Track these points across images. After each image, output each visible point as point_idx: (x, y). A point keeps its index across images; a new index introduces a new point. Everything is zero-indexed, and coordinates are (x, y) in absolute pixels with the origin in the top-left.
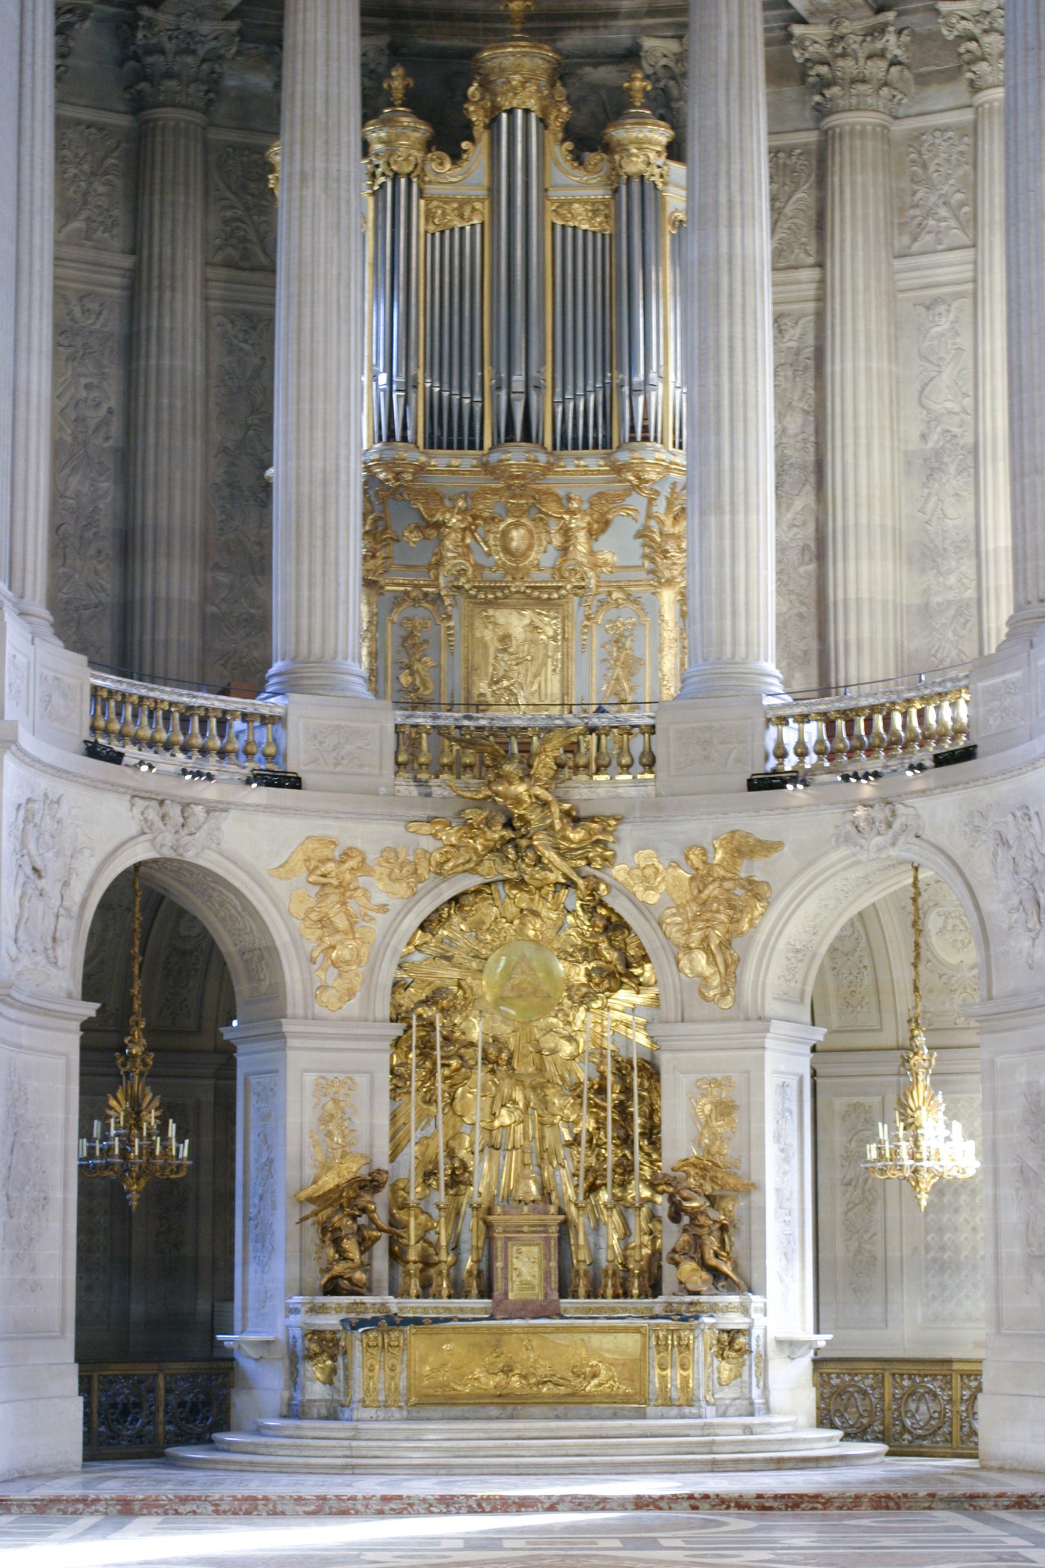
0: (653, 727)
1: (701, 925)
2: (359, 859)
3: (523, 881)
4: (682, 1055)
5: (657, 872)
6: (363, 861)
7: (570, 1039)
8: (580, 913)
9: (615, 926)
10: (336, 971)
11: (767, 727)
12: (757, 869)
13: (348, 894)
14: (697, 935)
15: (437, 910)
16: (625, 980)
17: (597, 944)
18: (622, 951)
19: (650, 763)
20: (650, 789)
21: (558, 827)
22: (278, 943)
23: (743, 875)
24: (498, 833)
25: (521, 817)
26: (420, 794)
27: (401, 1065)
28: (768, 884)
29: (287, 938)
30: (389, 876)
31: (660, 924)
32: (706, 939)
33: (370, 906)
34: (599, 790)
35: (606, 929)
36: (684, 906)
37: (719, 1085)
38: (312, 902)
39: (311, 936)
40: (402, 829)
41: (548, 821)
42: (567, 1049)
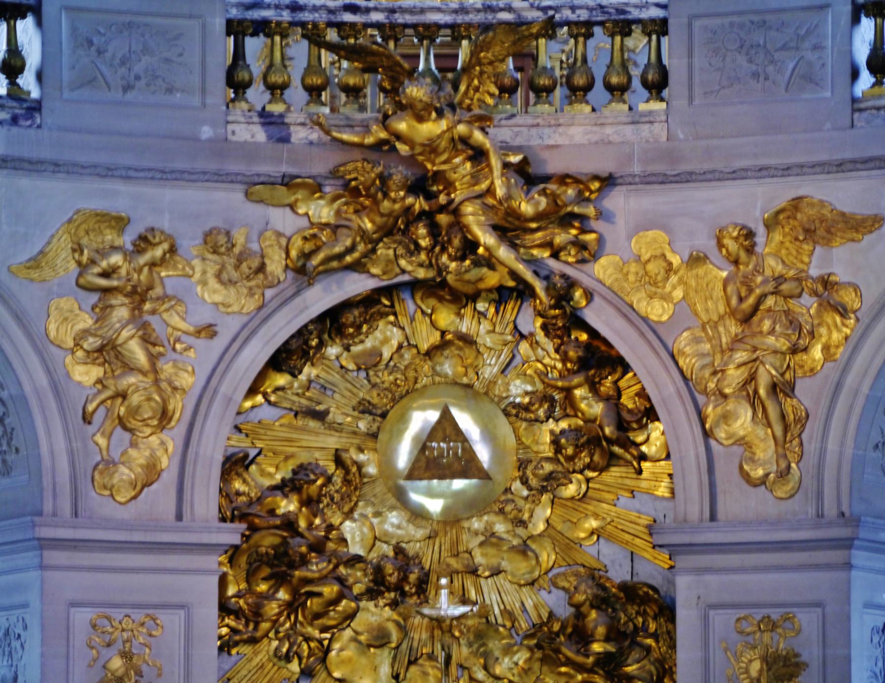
0: (664, 22)
1: (741, 356)
2: (166, 246)
3: (444, 284)
4: (709, 578)
5: (670, 269)
6: (173, 250)
7: (523, 550)
8: (540, 336)
9: (599, 360)
10: (127, 435)
11: (856, 21)
12: (838, 260)
13: (147, 306)
14: (735, 376)
15: (302, 333)
16: (616, 449)
17: (568, 392)
18: (614, 400)
19: (657, 85)
20: (659, 131)
21: (500, 192)
22: (28, 388)
23: (814, 272)
24: (401, 199)
25: (438, 176)
26: (270, 137)
27: (238, 595)
28: (856, 288)
29: (43, 380)
30: (218, 276)
31: (673, 356)
32: (752, 378)
33: (183, 325)
34: (573, 130)
35: (583, 365)
36: (715, 327)
37: (773, 626)
38: (86, 321)
39: (85, 375)
40: (240, 196)
41: (484, 186)
42: (520, 567)
